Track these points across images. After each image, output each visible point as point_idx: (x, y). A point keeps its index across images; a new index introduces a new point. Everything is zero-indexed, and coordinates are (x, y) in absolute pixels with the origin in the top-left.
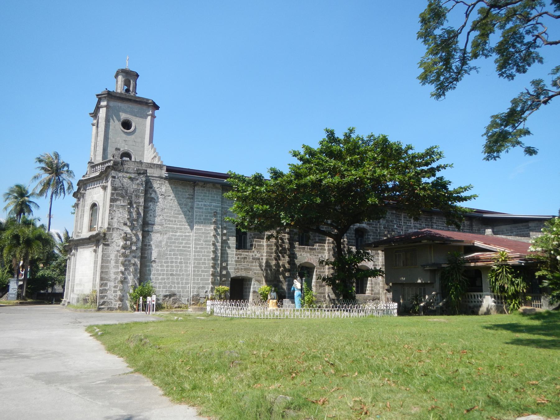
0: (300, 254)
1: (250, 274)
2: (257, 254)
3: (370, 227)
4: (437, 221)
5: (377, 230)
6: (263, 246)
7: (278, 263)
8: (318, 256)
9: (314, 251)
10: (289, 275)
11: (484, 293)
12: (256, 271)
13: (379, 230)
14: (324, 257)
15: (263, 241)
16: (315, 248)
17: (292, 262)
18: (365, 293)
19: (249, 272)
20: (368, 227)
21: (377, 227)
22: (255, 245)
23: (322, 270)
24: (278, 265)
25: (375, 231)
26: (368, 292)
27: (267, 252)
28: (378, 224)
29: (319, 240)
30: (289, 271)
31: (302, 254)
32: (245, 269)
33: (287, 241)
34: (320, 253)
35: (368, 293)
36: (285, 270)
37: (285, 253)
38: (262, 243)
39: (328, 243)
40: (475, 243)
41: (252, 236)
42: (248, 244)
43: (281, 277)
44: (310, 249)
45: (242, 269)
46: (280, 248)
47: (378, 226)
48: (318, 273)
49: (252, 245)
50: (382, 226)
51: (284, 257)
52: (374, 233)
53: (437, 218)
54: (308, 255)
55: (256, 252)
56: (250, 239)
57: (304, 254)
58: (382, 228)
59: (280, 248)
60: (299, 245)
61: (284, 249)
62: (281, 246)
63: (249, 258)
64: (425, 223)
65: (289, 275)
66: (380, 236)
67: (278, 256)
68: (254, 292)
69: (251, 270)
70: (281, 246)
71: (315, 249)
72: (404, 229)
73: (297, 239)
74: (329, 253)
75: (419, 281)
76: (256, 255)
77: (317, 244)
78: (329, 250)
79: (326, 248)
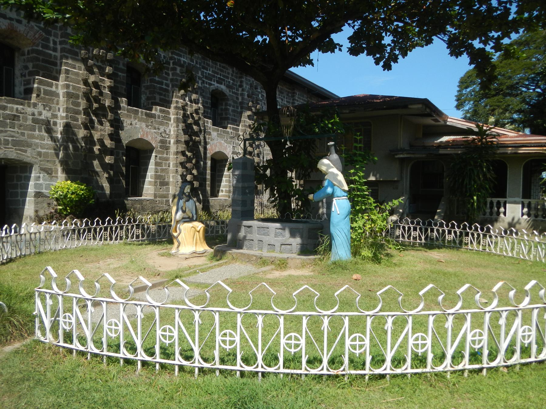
0: (129, 122)
1: (28, 156)
2: (44, 112)
3: (230, 91)
4: (299, 98)
5: (237, 98)
6: (58, 95)
7: (91, 136)
8: (159, 129)
9: (153, 120)
10: (112, 162)
11: (508, 199)
12: (42, 148)
13: (240, 98)
14: (168, 132)
16: (155, 114)
17: (115, 137)
18: (217, 196)
19: (25, 151)
20: (228, 91)
21: (237, 94)
22: (39, 89)
23: (165, 156)
24: (89, 140)
25: (235, 99)
26: (224, 193)
27: (67, 110)
28: (240, 89)
29: (161, 100)
30: (111, 152)
31: (134, 123)
32: (16, 143)
33: (106, 91)
34: (162, 124)
35: (222, 196)
37: (105, 116)
38: (54, 89)
39: (176, 108)
41: (31, 69)
42: (19, 88)
43: (96, 163)
44: (147, 114)
45: (7, 142)
46: (95, 105)
47: (240, 92)
48: (158, 160)
49: (28, 92)
50: (246, 94)
51: (101, 124)
52: (235, 102)
53: (299, 94)
54: (144, 125)
55: (40, 107)
56: (23, 75)
57: (137, 124)
58: (246, 97)
59: (95, 105)
60: (129, 104)
61: (102, 107)
62: (97, 100)
63: (26, 119)
64: (287, 99)
65: (112, 162)
66: (242, 108)
67: (92, 122)
68: (38, 195)
69: (29, 145)
70: (97, 100)
71: (153, 116)
73: (124, 92)
74: (177, 126)
76: (40, 114)
77: (158, 108)
78: (177, 120)
79: (172, 117)
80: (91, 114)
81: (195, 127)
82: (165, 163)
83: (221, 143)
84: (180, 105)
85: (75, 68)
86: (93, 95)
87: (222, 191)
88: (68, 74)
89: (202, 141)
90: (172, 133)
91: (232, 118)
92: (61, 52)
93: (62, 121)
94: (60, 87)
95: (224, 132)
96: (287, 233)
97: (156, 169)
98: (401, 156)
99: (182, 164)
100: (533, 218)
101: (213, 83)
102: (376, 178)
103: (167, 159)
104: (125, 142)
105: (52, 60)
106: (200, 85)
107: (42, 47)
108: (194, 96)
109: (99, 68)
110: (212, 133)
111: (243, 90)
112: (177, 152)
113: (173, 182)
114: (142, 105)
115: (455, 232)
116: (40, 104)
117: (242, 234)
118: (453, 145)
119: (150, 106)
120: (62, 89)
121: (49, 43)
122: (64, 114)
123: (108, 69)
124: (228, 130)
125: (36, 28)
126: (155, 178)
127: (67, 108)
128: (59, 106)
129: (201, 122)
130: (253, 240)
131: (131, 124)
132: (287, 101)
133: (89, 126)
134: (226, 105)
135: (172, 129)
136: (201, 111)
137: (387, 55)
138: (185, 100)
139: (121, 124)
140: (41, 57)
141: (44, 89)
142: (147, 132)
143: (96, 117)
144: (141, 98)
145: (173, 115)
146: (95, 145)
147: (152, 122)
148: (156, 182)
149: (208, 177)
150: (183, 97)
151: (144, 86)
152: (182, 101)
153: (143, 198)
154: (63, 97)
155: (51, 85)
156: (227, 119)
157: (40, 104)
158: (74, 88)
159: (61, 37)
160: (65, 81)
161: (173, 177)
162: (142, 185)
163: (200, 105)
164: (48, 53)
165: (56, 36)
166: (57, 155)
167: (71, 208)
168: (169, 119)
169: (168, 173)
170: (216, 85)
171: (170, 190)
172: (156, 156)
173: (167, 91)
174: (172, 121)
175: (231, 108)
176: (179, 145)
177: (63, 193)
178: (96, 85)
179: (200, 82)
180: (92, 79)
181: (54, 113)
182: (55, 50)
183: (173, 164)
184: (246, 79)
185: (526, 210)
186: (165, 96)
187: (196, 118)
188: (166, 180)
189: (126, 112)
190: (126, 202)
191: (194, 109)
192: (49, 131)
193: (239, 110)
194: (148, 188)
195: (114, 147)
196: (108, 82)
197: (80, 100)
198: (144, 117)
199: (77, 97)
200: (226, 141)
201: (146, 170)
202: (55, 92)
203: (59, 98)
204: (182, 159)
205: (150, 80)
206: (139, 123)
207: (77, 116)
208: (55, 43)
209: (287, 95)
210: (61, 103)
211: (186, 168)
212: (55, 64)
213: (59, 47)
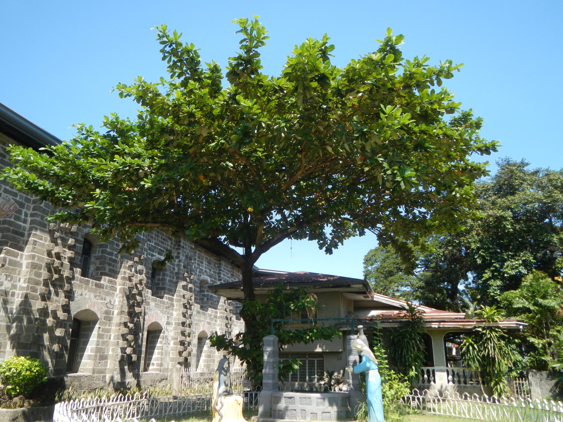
0: (80, 293)
4: (225, 269)
5: (174, 269)
6: (20, 265)
8: (105, 299)
11: (436, 368)
14: (112, 303)
15: (22, 255)
16: (103, 285)
23: (107, 327)
24: (44, 312)
25: (172, 270)
26: (155, 367)
27: (30, 281)
28: (177, 260)
29: (110, 270)
31: (84, 293)
33: (66, 262)
34: (108, 294)
36: (59, 323)
37: (62, 287)
38: (18, 259)
39: (124, 278)
40: (375, 296)
43: (46, 336)
44: (97, 285)
46: (56, 276)
47: (176, 263)
48: (101, 332)
51: (57, 294)
52: (171, 272)
54: (92, 295)
58: (182, 268)
61: (61, 278)
65: (62, 334)
66: (178, 278)
70: (57, 271)
72: (198, 273)
73: (79, 263)
75: (319, 350)
77: (107, 278)
79: (118, 287)
80: (50, 285)
81: (138, 298)
82: (107, 335)
83: (157, 313)
84: (127, 276)
85: (41, 239)
86: (55, 265)
87: (153, 364)
88: (35, 245)
89: (143, 312)
90: (117, 303)
91: (168, 288)
92: (31, 224)
93: (21, 292)
94: (24, 257)
95: (161, 302)
96: (327, 403)
97: (98, 341)
98: (346, 329)
99: (123, 335)
100: (457, 384)
101: (155, 254)
102: (323, 350)
103: (109, 331)
104: (73, 313)
105: (21, 231)
106: (145, 256)
107: (14, 219)
108: (140, 267)
109: (63, 239)
110: (151, 303)
111: (180, 261)
112: (121, 323)
113: (113, 355)
114: (90, 275)
115: (418, 399)
116: (3, 274)
117: (282, 405)
118: (384, 319)
119: (99, 276)
120: (25, 259)
121: (21, 215)
122: (26, 285)
123: (71, 241)
124: (164, 300)
125: (12, 200)
126: (96, 352)
127: (29, 279)
128: (20, 276)
129: (143, 292)
130: (295, 410)
131: (81, 295)
132: (214, 272)
133: (45, 297)
134: (164, 275)
135: (117, 300)
136: (144, 282)
137: (329, 242)
138: (131, 271)
139: (72, 295)
140: (12, 228)
141: (10, 260)
142: (95, 303)
143: (54, 287)
144: (89, 268)
145: (120, 285)
146: (48, 317)
147: (100, 293)
148: (96, 356)
149: (144, 349)
150: (130, 267)
151: (94, 257)
152: (129, 271)
153: (79, 374)
154: (27, 268)
155: (16, 256)
156: (164, 289)
157: (3, 274)
158: (39, 259)
159: (34, 210)
160: (32, 252)
161: (113, 350)
162: (79, 360)
163: (143, 275)
164: (18, 224)
165: (28, 208)
166: (9, 328)
167: (20, 387)
168: (115, 290)
169: (108, 346)
170: (157, 256)
171: (109, 364)
172: (100, 328)
173: (115, 261)
174: (118, 292)
175: (168, 278)
176: (123, 316)
177: (16, 370)
178: (58, 256)
179: (145, 253)
180: (56, 250)
181: (14, 284)
182: (25, 221)
183: (114, 336)
184: (183, 251)
185: (450, 377)
186: (113, 266)
187: (140, 289)
188: (106, 353)
189: (78, 283)
190: (65, 379)
191: (139, 279)
192: (5, 302)
193: (175, 280)
194: (86, 363)
195: (66, 319)
196: (69, 254)
197: (42, 271)
198: (94, 287)
199: (40, 269)
200: (162, 312)
201: (86, 343)
202: (19, 262)
203: (22, 268)
204: (126, 331)
205: (102, 251)
206: (89, 293)
207: (37, 286)
208: (26, 215)
209: (214, 266)
210: (23, 273)
211: (127, 340)
212: (22, 235)
213: (29, 219)
